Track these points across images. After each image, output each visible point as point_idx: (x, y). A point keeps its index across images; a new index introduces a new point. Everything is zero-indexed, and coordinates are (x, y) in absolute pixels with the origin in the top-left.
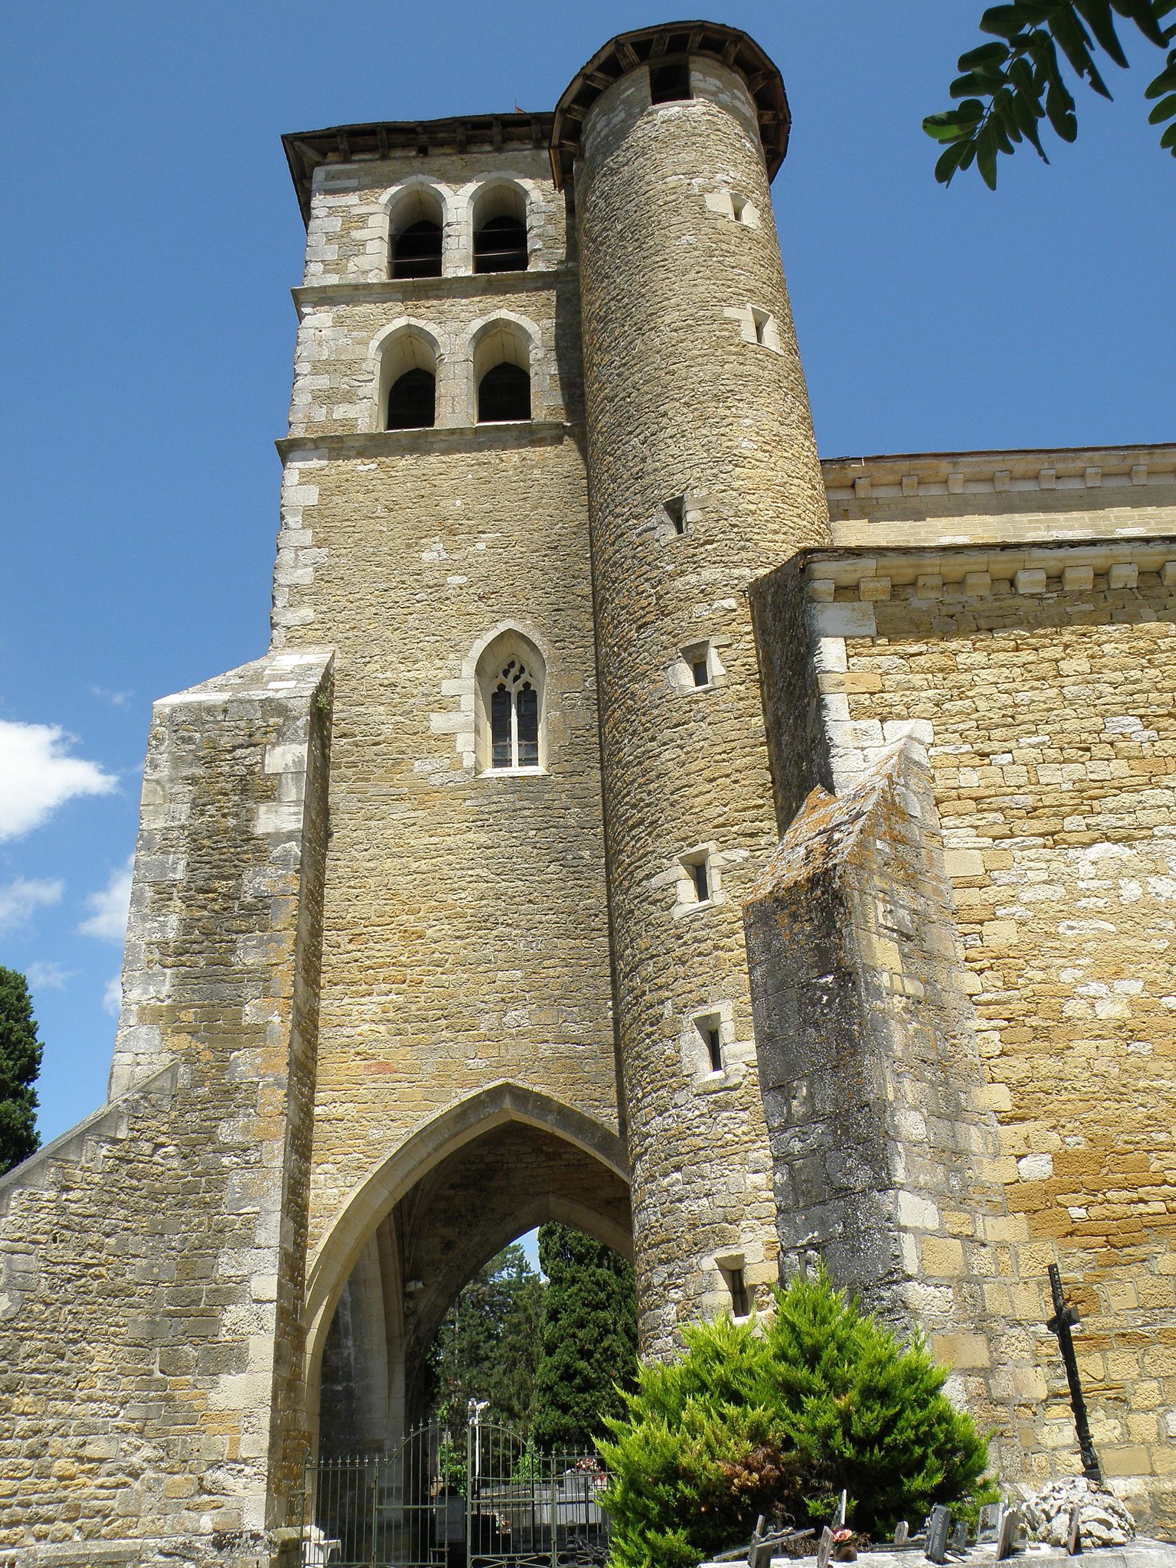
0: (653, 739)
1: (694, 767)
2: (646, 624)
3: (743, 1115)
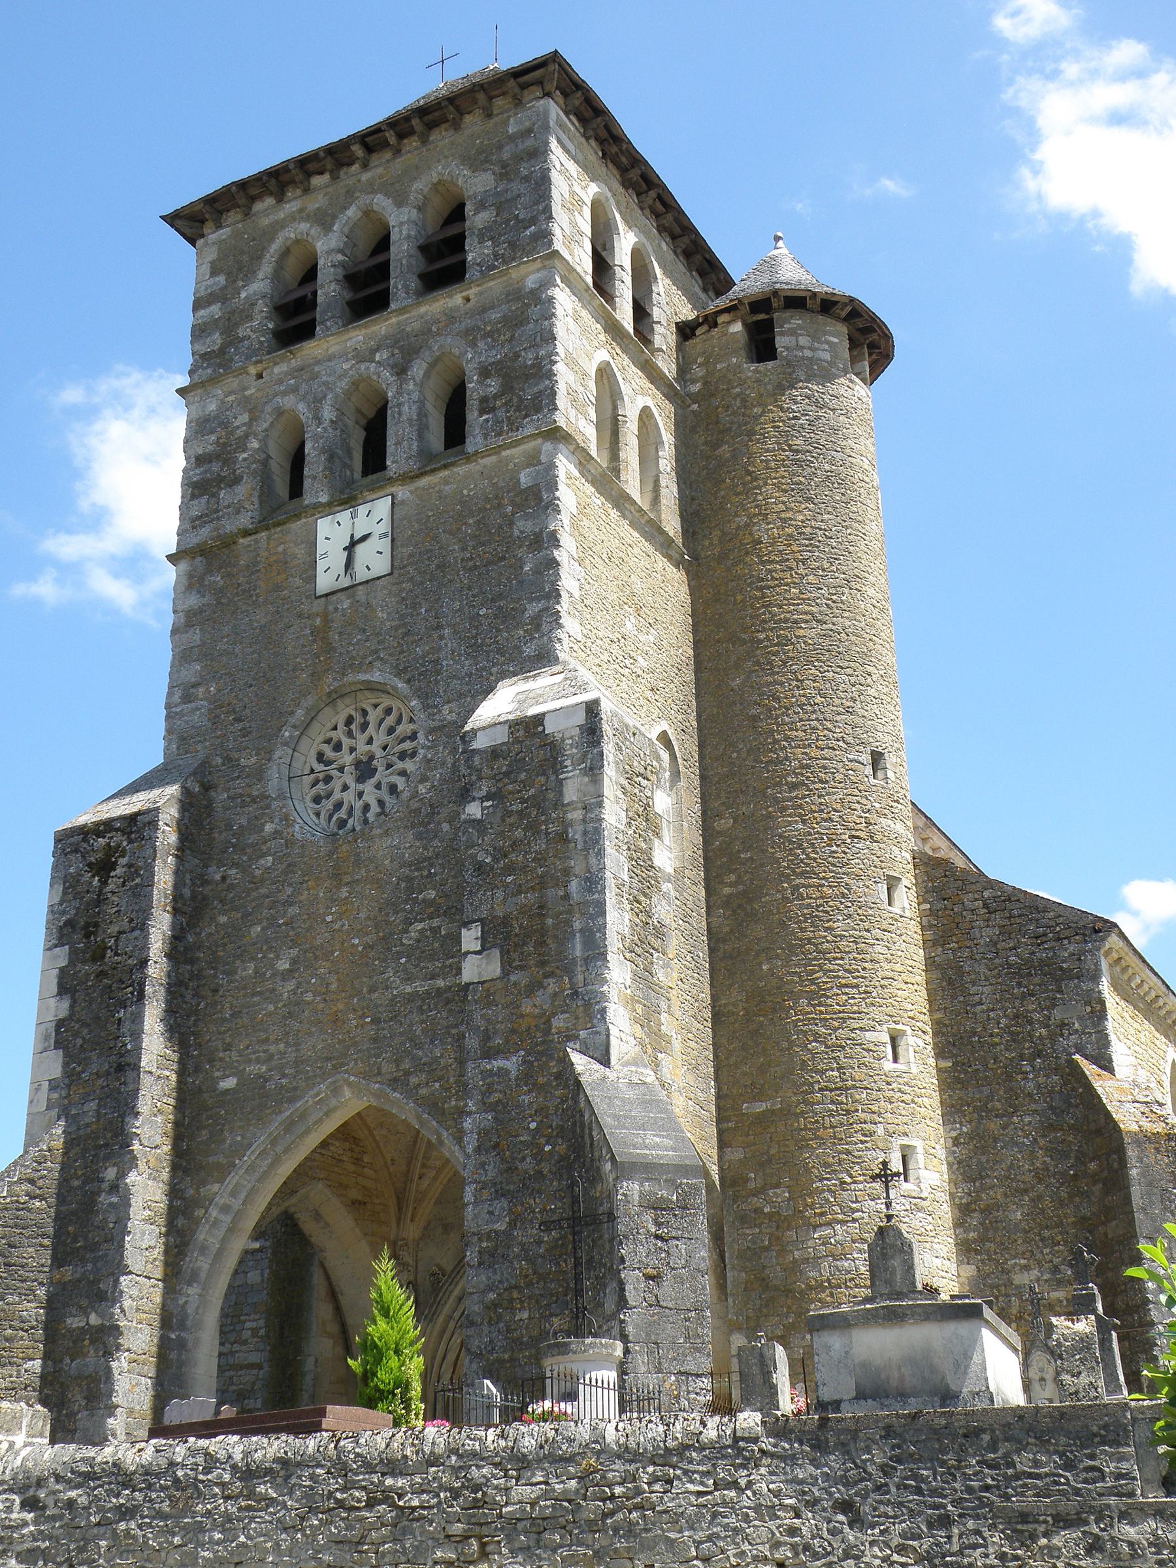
0: (868, 931)
1: (898, 967)
2: (858, 837)
3: (930, 1218)
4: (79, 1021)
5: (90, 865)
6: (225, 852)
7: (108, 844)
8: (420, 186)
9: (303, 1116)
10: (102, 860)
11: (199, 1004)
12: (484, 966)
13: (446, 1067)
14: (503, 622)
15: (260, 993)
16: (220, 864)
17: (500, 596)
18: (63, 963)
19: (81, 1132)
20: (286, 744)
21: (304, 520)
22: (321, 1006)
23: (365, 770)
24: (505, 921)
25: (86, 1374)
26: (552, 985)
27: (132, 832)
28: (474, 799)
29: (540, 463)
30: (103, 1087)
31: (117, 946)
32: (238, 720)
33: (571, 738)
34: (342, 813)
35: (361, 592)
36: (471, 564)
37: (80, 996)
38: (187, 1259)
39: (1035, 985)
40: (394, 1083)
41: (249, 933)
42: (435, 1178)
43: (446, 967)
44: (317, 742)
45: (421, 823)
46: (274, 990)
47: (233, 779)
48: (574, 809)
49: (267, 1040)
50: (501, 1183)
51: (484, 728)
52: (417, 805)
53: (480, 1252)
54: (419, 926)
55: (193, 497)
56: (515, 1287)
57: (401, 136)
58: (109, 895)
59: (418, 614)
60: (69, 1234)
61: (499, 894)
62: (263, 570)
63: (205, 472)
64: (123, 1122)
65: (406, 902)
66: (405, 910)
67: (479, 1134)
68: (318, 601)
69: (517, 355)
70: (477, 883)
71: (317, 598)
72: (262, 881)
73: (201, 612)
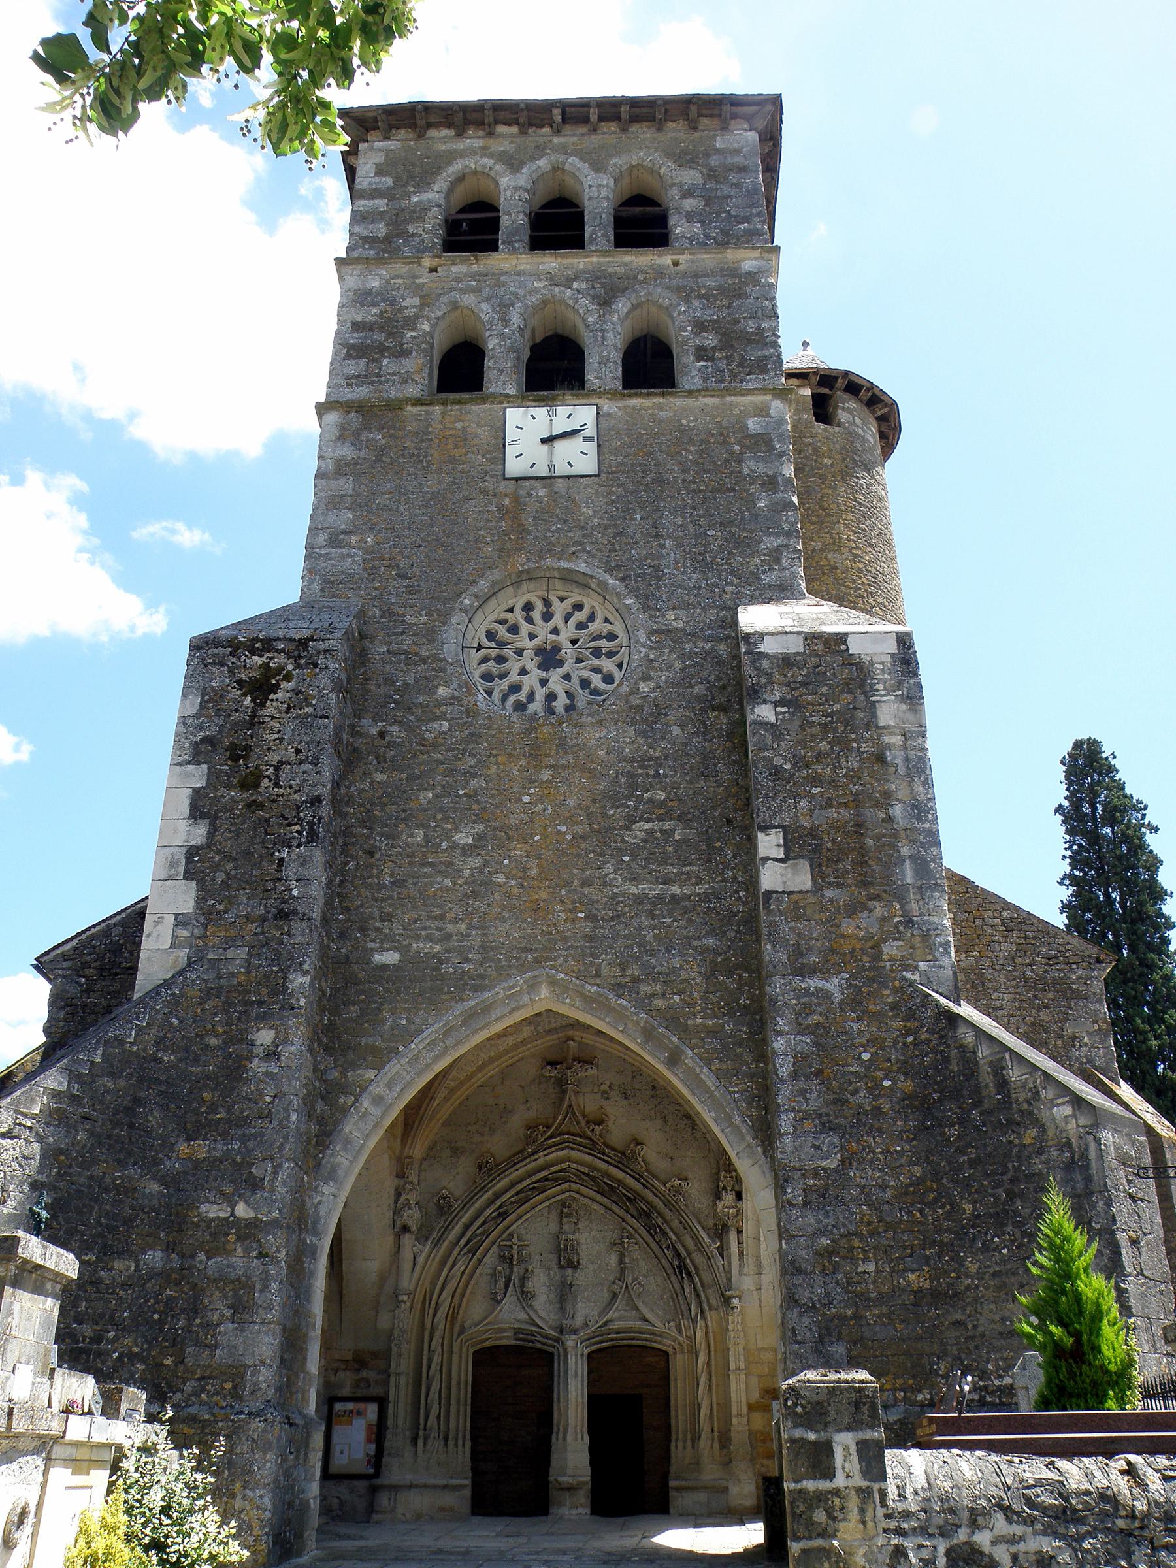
4: (219, 852)
5: (240, 683)
6: (385, 707)
7: (266, 666)
8: (620, 162)
9: (487, 1008)
10: (257, 680)
11: (346, 864)
12: (789, 876)
13: (688, 980)
14: (736, 548)
15: (432, 865)
16: (376, 718)
17: (731, 523)
18: (200, 783)
19: (223, 982)
20: (466, 612)
21: (488, 406)
22: (516, 891)
23: (549, 658)
24: (813, 833)
25: (232, 1276)
26: (879, 909)
27: (300, 657)
28: (765, 702)
29: (768, 415)
30: (256, 934)
31: (277, 776)
32: (404, 576)
33: (882, 663)
34: (522, 696)
35: (560, 485)
36: (693, 486)
37: (223, 824)
38: (329, 1152)
39: (1049, 999)
40: (619, 988)
41: (417, 798)
42: (446, 1099)
43: (682, 874)
44: (488, 619)
45: (645, 721)
46: (452, 864)
47: (395, 634)
48: (891, 734)
49: (442, 917)
50: (828, 1115)
51: (773, 634)
52: (639, 702)
53: (804, 1190)
54: (647, 826)
55: (348, 356)
56: (856, 1234)
57: (601, 119)
58: (267, 719)
59: (632, 519)
60: (203, 1101)
61: (804, 804)
62: (436, 441)
63: (366, 338)
64: (285, 978)
65: (629, 798)
66: (628, 807)
67: (795, 1057)
68: (508, 482)
69: (736, 321)
70: (774, 788)
71: (506, 479)
72: (435, 745)
73: (356, 464)
